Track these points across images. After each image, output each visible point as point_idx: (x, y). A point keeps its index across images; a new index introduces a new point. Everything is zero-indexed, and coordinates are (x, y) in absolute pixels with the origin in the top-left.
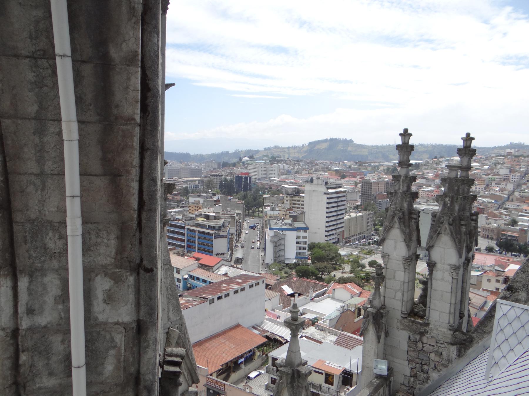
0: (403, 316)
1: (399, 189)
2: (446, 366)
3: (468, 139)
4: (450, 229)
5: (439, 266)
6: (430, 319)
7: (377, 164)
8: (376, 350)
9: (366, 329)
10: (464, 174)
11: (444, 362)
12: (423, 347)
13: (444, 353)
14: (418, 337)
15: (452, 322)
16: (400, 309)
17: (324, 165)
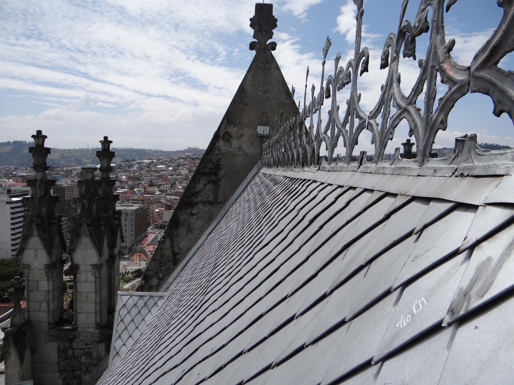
0: (50, 327)
1: (36, 194)
2: (96, 365)
3: (106, 142)
4: (89, 230)
5: (82, 268)
6: (78, 323)
7: (70, 168)
8: (21, 372)
9: (7, 352)
10: (105, 175)
11: (94, 362)
12: (74, 353)
13: (94, 354)
14: (67, 344)
15: (98, 320)
16: (47, 320)
17: (6, 170)
